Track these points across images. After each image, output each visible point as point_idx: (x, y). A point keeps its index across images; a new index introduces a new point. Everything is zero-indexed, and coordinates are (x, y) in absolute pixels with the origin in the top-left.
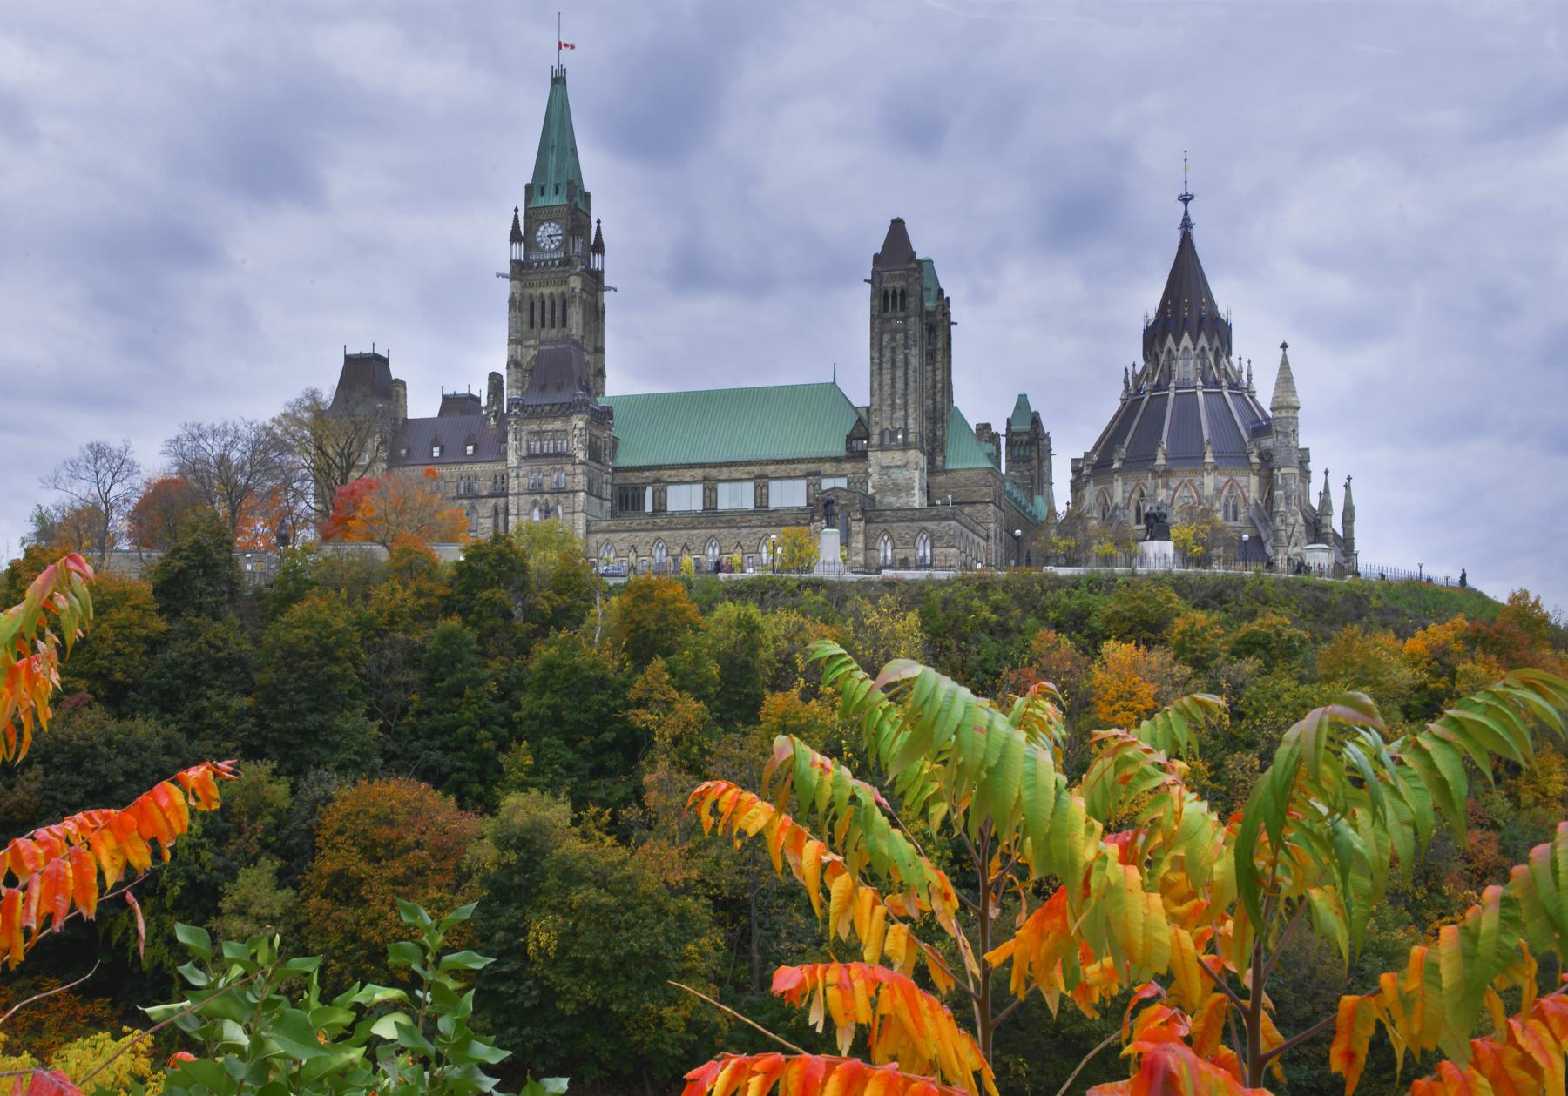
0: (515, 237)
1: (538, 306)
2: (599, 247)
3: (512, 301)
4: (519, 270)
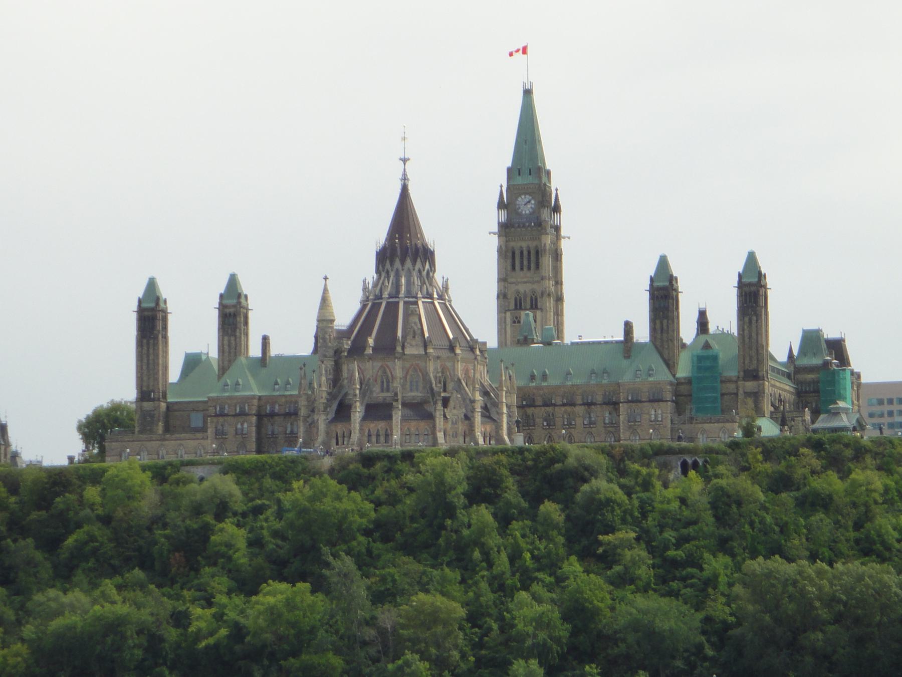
0: (501, 205)
2: (557, 209)
3: (500, 251)
4: (505, 229)
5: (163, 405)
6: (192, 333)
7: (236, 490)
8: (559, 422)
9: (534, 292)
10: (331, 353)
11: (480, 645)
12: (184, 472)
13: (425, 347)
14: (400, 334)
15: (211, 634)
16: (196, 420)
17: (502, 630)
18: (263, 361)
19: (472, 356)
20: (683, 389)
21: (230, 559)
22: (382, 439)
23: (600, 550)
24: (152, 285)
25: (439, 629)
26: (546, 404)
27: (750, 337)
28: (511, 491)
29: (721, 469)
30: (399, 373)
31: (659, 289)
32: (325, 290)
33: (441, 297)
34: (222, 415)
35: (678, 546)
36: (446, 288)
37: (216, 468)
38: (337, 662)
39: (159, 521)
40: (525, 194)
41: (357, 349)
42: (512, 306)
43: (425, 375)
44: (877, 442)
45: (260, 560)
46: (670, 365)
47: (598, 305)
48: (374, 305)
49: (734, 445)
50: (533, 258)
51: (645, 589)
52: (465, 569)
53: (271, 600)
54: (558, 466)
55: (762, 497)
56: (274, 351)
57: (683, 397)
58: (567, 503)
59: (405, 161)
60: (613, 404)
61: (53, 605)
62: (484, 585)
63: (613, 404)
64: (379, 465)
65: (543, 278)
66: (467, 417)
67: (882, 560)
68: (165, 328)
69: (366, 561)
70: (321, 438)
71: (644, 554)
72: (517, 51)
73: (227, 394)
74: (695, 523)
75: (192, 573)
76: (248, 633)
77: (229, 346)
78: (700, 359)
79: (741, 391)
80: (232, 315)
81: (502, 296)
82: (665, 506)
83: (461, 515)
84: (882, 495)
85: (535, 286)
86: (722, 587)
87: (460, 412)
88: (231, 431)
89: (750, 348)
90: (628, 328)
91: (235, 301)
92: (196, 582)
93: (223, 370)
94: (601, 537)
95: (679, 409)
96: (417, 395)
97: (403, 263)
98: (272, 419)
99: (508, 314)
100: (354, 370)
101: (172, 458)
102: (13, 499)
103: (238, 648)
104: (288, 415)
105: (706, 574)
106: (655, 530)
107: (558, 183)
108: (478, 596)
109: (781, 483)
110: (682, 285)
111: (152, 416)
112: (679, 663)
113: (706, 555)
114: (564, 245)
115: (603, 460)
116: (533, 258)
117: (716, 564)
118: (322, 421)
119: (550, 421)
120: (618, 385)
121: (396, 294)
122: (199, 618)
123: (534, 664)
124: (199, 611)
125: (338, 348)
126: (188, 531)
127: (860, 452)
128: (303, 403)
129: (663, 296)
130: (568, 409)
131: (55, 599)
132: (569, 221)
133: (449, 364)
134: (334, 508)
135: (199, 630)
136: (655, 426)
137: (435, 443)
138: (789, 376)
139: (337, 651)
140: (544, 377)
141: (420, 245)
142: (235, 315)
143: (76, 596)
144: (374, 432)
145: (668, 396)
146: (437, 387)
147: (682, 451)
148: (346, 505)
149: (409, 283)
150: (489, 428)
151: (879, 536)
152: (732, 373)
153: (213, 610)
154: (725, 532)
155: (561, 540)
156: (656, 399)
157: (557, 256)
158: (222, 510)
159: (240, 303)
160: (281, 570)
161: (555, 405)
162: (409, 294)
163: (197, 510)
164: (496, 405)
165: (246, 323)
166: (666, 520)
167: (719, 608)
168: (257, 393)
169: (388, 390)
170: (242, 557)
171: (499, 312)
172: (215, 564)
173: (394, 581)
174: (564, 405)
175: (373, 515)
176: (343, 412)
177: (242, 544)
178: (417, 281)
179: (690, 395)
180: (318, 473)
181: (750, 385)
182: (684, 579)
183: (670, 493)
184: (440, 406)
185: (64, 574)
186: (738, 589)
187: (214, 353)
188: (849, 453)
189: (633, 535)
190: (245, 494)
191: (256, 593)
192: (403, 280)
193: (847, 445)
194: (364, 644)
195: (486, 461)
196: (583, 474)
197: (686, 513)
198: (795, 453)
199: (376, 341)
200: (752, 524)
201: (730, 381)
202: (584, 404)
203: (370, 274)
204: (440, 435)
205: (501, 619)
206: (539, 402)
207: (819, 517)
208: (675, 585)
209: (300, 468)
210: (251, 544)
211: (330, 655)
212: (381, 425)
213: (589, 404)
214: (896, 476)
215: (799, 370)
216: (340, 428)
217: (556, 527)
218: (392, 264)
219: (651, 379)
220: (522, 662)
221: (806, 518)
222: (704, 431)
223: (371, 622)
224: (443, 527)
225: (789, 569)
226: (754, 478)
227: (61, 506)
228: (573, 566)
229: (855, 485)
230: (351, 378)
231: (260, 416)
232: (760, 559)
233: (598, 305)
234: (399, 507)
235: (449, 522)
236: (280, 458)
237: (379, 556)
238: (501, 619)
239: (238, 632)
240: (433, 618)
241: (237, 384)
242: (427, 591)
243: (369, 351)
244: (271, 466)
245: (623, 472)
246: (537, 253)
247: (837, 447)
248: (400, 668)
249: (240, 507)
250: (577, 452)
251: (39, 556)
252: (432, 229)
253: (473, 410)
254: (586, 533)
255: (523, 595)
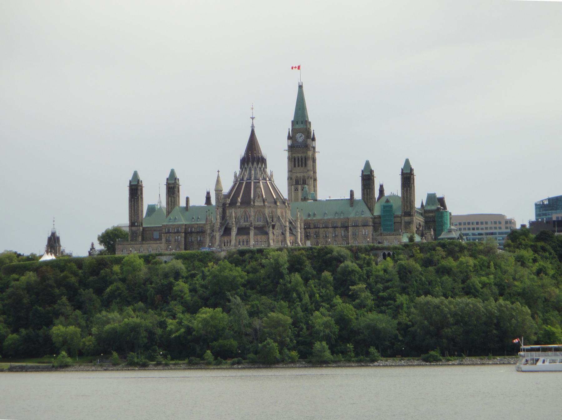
0: (289, 138)
1: (297, 159)
2: (314, 139)
3: (289, 158)
4: (291, 148)
5: (141, 228)
6: (154, 195)
7: (183, 267)
8: (321, 236)
9: (304, 176)
10: (221, 205)
11: (298, 335)
12: (157, 258)
13: (264, 202)
14: (252, 196)
15: (177, 331)
16: (156, 235)
17: (308, 329)
18: (187, 208)
19: (283, 205)
20: (377, 220)
21: (182, 298)
22: (245, 243)
23: (350, 293)
24: (135, 175)
25: (281, 329)
26: (315, 228)
27: (407, 197)
28: (308, 267)
29: (401, 256)
30: (252, 214)
31: (366, 175)
32: (218, 177)
33: (270, 180)
34: (169, 232)
35: (384, 291)
36: (272, 176)
37: (171, 257)
38: (235, 343)
39: (148, 281)
40: (300, 132)
41: (233, 203)
42: (294, 183)
43: (264, 214)
44: (469, 244)
45: (196, 298)
46: (371, 210)
47: (335, 183)
48: (240, 183)
49: (406, 246)
50: (303, 161)
51: (371, 310)
52: (289, 301)
53: (204, 316)
54: (329, 255)
55: (420, 269)
56: (191, 204)
57: (377, 224)
58: (333, 272)
59: (253, 118)
60: (346, 228)
61: (105, 318)
62: (299, 309)
63: (346, 228)
64: (247, 255)
65: (308, 171)
66: (283, 234)
67: (475, 296)
68: (142, 194)
69: (245, 298)
70: (217, 243)
71: (369, 294)
72: (295, 67)
73: (171, 223)
74: (391, 280)
75: (165, 304)
76: (194, 330)
77: (171, 201)
78: (385, 207)
79: (403, 221)
80: (172, 188)
81: (290, 178)
82: (377, 273)
83: (287, 277)
84: (473, 268)
85: (305, 174)
86: (405, 309)
87: (280, 231)
88: (173, 240)
89: (407, 202)
90: (352, 193)
91: (173, 182)
92: (167, 308)
93: (169, 213)
94: (351, 287)
95: (375, 229)
96: (260, 223)
97: (253, 164)
98: (192, 234)
99: (293, 187)
100: (232, 213)
101: (153, 252)
102: (80, 271)
103: (189, 337)
104: (198, 233)
105: (398, 302)
106: (373, 284)
107: (314, 128)
108: (296, 313)
109: (427, 263)
110: (375, 174)
111: (137, 234)
112: (387, 343)
113: (397, 295)
114: (317, 155)
115: (349, 252)
116: (303, 161)
117: (402, 299)
118: (218, 235)
119: (317, 235)
120: (348, 219)
121: (250, 178)
122: (171, 324)
123: (324, 343)
124: (171, 321)
125: (228, 202)
126: (162, 285)
127: (462, 249)
128: (208, 228)
129: (368, 178)
130: (326, 229)
131: (106, 316)
132: (319, 144)
133: (274, 210)
134: (230, 275)
135: (172, 329)
136: (365, 238)
137: (269, 245)
138: (421, 214)
139: (235, 339)
140: (314, 215)
141: (260, 156)
142: (174, 188)
143: (115, 315)
144: (241, 240)
145: (371, 224)
146: (269, 220)
147: (383, 248)
148: (235, 273)
149: (256, 174)
150: (293, 238)
151: (474, 286)
152: (399, 213)
153: (177, 320)
154: (404, 285)
155: (332, 288)
156: (365, 225)
157: (314, 160)
158: (177, 275)
159: (176, 182)
160: (206, 302)
161: (319, 228)
162: (255, 178)
163: (166, 275)
164: (295, 228)
165: (179, 191)
166: (379, 280)
167: (403, 318)
168: (184, 222)
169: (247, 222)
170: (188, 296)
171: (289, 186)
172: (175, 300)
173: (258, 307)
174: (323, 228)
175: (246, 278)
176: (227, 231)
177: (187, 291)
178: (259, 173)
179: (380, 223)
180: (219, 259)
181: (407, 219)
182: (387, 305)
183: (379, 267)
184: (271, 228)
185: (107, 305)
186: (413, 310)
187: (164, 204)
188: (457, 249)
189: (365, 286)
190: (187, 268)
191: (196, 313)
192: (253, 172)
193: (456, 246)
194: (246, 335)
195: (296, 253)
196: (340, 259)
197: (387, 276)
198: (434, 250)
199: (241, 199)
200: (416, 281)
201: (397, 217)
202: (332, 227)
203: (238, 170)
204: (271, 242)
205: (307, 323)
206: (312, 226)
207: (445, 278)
208: (383, 308)
209: (211, 257)
210: (191, 291)
211: (232, 340)
212: (245, 237)
213: (335, 227)
214: (479, 260)
215: (426, 212)
216: (226, 239)
217: (329, 282)
218: (248, 165)
219: (363, 216)
220: (319, 343)
221: (440, 278)
222: (387, 239)
223: (250, 325)
224: (278, 283)
225: (436, 301)
226: (416, 260)
227: (103, 274)
228: (338, 300)
229: (462, 263)
230: (231, 216)
231: (186, 233)
232: (423, 297)
233: (335, 183)
234: (258, 274)
235: (281, 281)
236: (201, 252)
237: (250, 296)
238: (307, 323)
239: (189, 330)
240: (278, 323)
241: (176, 219)
242: (273, 312)
243: (239, 204)
244: (197, 256)
245: (357, 258)
246: (305, 159)
247: (452, 246)
248: (265, 346)
249: (185, 274)
250: (338, 249)
251: (94, 296)
252: (265, 149)
253: (285, 231)
254: (343, 285)
255: (317, 313)
